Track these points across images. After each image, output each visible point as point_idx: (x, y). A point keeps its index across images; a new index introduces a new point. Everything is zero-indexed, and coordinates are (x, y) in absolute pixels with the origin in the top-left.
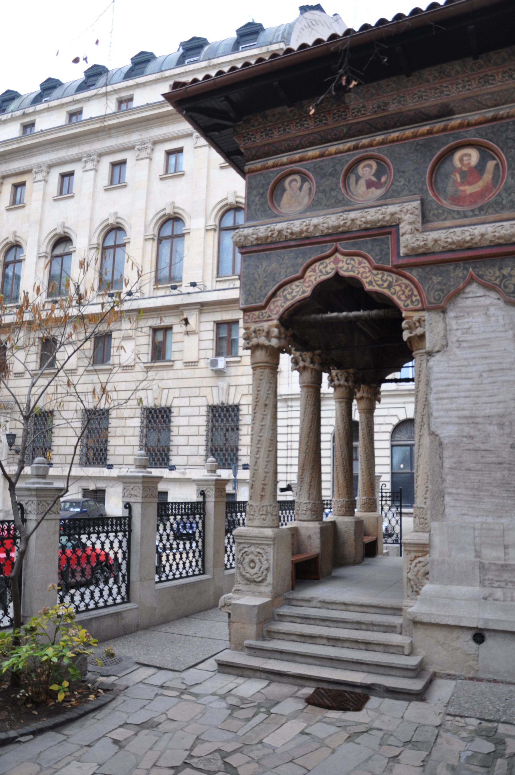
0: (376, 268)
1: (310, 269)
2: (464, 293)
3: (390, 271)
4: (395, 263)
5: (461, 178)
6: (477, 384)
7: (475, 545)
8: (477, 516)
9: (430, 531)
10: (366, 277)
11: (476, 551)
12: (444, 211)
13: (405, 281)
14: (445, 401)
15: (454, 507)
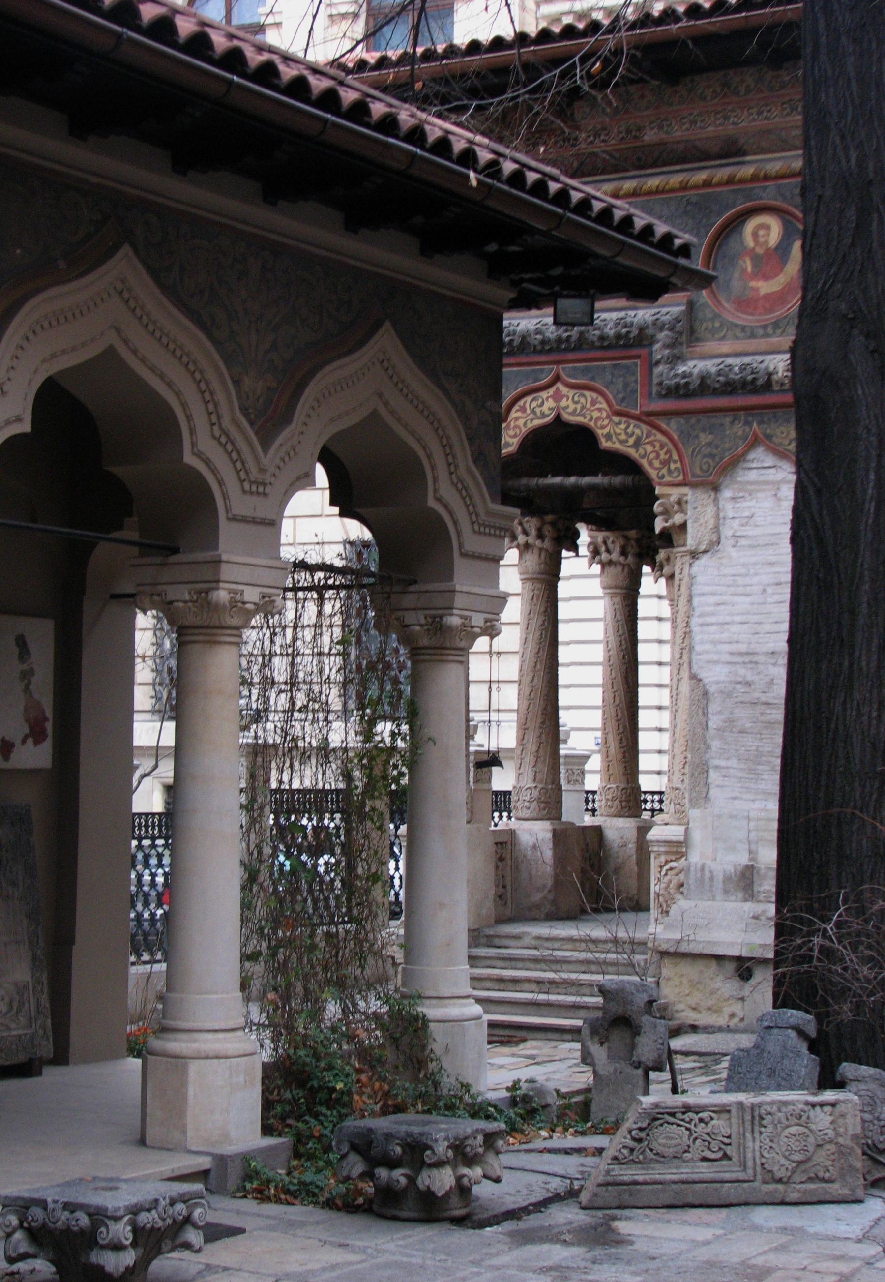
0: (618, 413)
1: (516, 407)
2: (745, 461)
3: (637, 418)
4: (645, 409)
5: (754, 266)
6: (758, 604)
7: (749, 842)
8: (753, 800)
9: (688, 823)
10: (603, 427)
11: (750, 852)
12: (722, 325)
13: (659, 436)
14: (713, 629)
15: (722, 787)
